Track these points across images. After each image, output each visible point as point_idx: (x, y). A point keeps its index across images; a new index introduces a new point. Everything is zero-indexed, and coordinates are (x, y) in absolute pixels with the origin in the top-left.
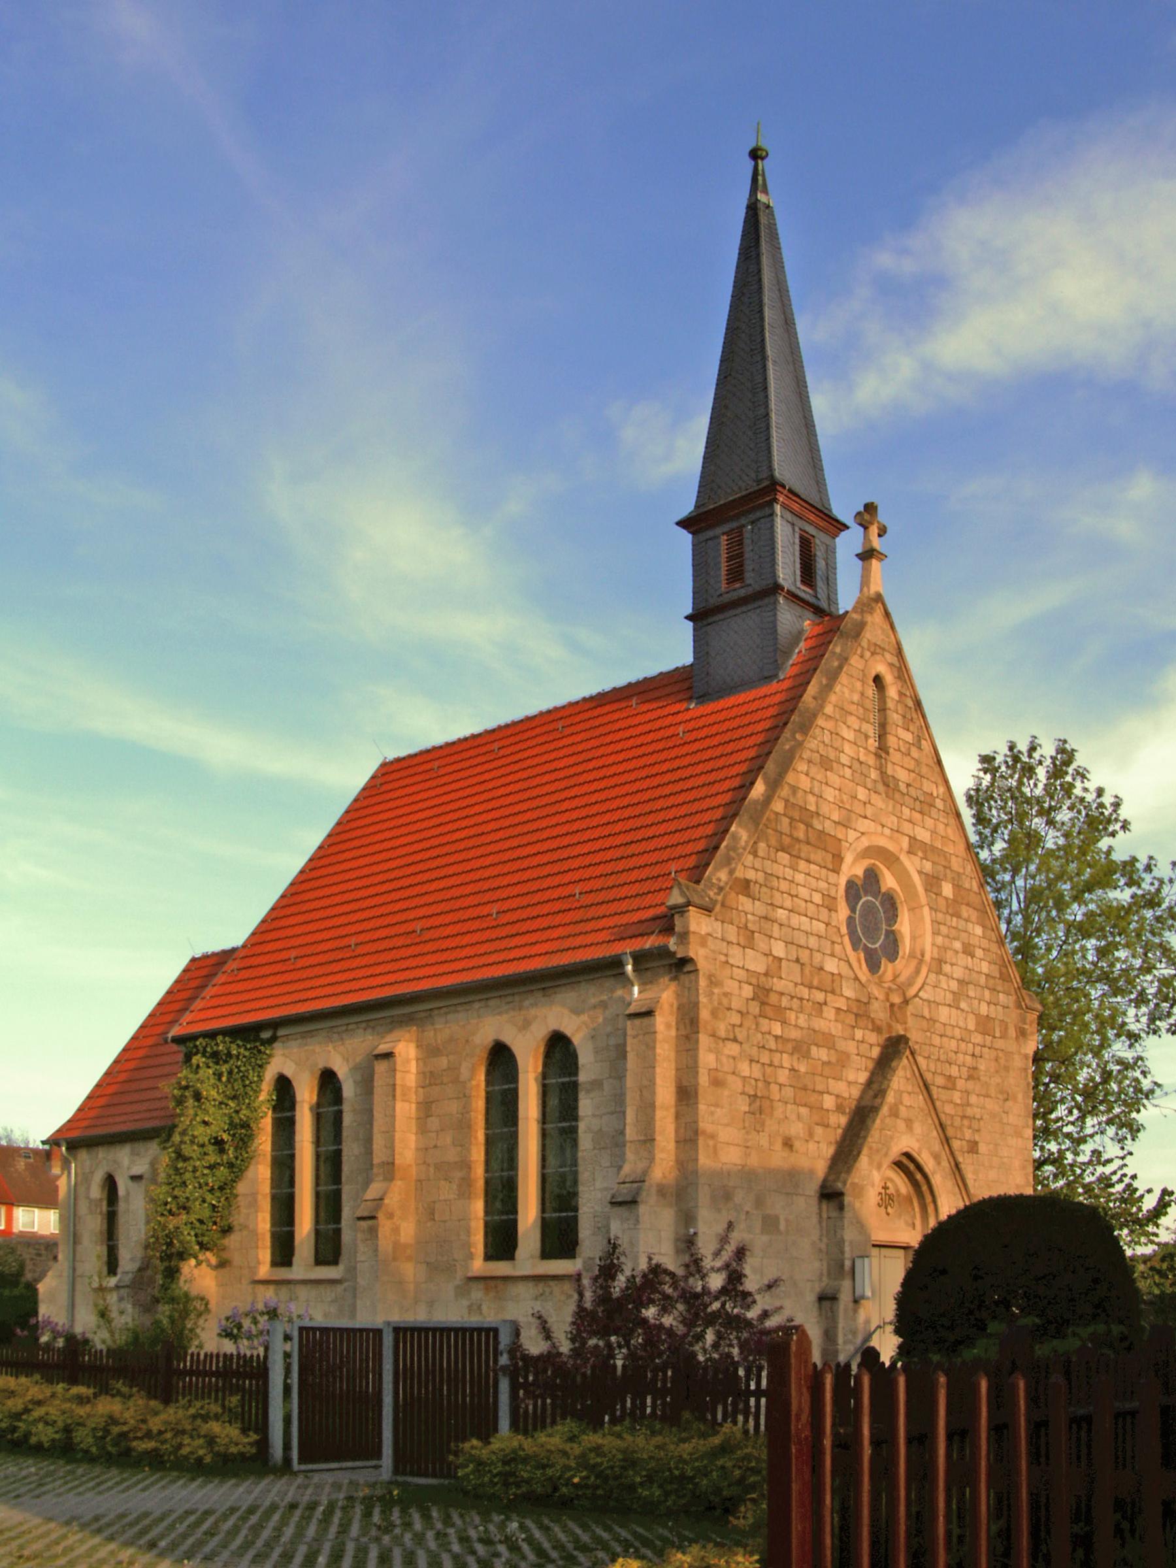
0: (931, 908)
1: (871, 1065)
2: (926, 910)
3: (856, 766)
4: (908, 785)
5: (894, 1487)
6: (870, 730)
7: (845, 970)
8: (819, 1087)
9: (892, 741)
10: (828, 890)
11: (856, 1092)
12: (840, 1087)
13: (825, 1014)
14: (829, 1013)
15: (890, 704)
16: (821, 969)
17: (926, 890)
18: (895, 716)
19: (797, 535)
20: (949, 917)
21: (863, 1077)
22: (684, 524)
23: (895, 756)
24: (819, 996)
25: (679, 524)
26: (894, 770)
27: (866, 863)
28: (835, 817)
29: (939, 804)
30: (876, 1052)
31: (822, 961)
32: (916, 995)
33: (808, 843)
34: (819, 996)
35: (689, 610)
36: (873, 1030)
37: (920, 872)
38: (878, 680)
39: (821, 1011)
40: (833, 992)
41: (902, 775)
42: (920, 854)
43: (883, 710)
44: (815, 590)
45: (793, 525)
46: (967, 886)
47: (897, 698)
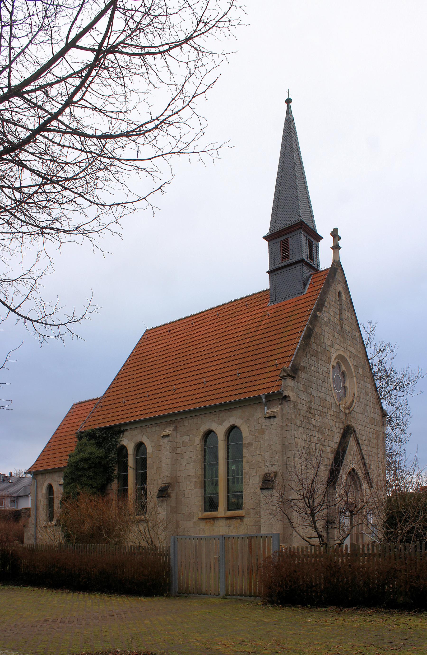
0: (356, 378)
1: (340, 436)
2: (355, 378)
3: (334, 324)
4: (349, 332)
5: (268, 548)
6: (337, 311)
7: (333, 401)
8: (326, 444)
9: (344, 316)
10: (327, 370)
11: (336, 446)
12: (331, 444)
13: (327, 417)
14: (328, 416)
15: (344, 303)
16: (326, 400)
17: (355, 371)
18: (345, 306)
19: (308, 241)
20: (361, 381)
21: (338, 440)
22: (265, 238)
23: (345, 321)
24: (325, 410)
25: (264, 238)
26: (345, 326)
27: (337, 361)
28: (329, 344)
29: (358, 339)
30: (342, 431)
31: (326, 397)
32: (353, 410)
33: (321, 353)
34: (325, 410)
35: (268, 269)
36: (341, 423)
37: (353, 364)
38: (340, 293)
39: (326, 415)
40: (329, 409)
41: (347, 328)
42: (353, 357)
43: (341, 305)
44: (314, 262)
45: (306, 237)
46: (366, 370)
47: (345, 300)
